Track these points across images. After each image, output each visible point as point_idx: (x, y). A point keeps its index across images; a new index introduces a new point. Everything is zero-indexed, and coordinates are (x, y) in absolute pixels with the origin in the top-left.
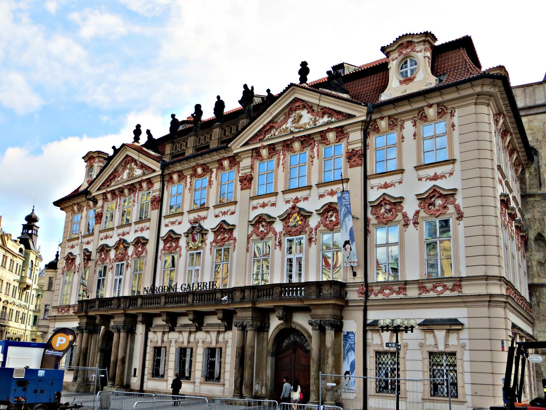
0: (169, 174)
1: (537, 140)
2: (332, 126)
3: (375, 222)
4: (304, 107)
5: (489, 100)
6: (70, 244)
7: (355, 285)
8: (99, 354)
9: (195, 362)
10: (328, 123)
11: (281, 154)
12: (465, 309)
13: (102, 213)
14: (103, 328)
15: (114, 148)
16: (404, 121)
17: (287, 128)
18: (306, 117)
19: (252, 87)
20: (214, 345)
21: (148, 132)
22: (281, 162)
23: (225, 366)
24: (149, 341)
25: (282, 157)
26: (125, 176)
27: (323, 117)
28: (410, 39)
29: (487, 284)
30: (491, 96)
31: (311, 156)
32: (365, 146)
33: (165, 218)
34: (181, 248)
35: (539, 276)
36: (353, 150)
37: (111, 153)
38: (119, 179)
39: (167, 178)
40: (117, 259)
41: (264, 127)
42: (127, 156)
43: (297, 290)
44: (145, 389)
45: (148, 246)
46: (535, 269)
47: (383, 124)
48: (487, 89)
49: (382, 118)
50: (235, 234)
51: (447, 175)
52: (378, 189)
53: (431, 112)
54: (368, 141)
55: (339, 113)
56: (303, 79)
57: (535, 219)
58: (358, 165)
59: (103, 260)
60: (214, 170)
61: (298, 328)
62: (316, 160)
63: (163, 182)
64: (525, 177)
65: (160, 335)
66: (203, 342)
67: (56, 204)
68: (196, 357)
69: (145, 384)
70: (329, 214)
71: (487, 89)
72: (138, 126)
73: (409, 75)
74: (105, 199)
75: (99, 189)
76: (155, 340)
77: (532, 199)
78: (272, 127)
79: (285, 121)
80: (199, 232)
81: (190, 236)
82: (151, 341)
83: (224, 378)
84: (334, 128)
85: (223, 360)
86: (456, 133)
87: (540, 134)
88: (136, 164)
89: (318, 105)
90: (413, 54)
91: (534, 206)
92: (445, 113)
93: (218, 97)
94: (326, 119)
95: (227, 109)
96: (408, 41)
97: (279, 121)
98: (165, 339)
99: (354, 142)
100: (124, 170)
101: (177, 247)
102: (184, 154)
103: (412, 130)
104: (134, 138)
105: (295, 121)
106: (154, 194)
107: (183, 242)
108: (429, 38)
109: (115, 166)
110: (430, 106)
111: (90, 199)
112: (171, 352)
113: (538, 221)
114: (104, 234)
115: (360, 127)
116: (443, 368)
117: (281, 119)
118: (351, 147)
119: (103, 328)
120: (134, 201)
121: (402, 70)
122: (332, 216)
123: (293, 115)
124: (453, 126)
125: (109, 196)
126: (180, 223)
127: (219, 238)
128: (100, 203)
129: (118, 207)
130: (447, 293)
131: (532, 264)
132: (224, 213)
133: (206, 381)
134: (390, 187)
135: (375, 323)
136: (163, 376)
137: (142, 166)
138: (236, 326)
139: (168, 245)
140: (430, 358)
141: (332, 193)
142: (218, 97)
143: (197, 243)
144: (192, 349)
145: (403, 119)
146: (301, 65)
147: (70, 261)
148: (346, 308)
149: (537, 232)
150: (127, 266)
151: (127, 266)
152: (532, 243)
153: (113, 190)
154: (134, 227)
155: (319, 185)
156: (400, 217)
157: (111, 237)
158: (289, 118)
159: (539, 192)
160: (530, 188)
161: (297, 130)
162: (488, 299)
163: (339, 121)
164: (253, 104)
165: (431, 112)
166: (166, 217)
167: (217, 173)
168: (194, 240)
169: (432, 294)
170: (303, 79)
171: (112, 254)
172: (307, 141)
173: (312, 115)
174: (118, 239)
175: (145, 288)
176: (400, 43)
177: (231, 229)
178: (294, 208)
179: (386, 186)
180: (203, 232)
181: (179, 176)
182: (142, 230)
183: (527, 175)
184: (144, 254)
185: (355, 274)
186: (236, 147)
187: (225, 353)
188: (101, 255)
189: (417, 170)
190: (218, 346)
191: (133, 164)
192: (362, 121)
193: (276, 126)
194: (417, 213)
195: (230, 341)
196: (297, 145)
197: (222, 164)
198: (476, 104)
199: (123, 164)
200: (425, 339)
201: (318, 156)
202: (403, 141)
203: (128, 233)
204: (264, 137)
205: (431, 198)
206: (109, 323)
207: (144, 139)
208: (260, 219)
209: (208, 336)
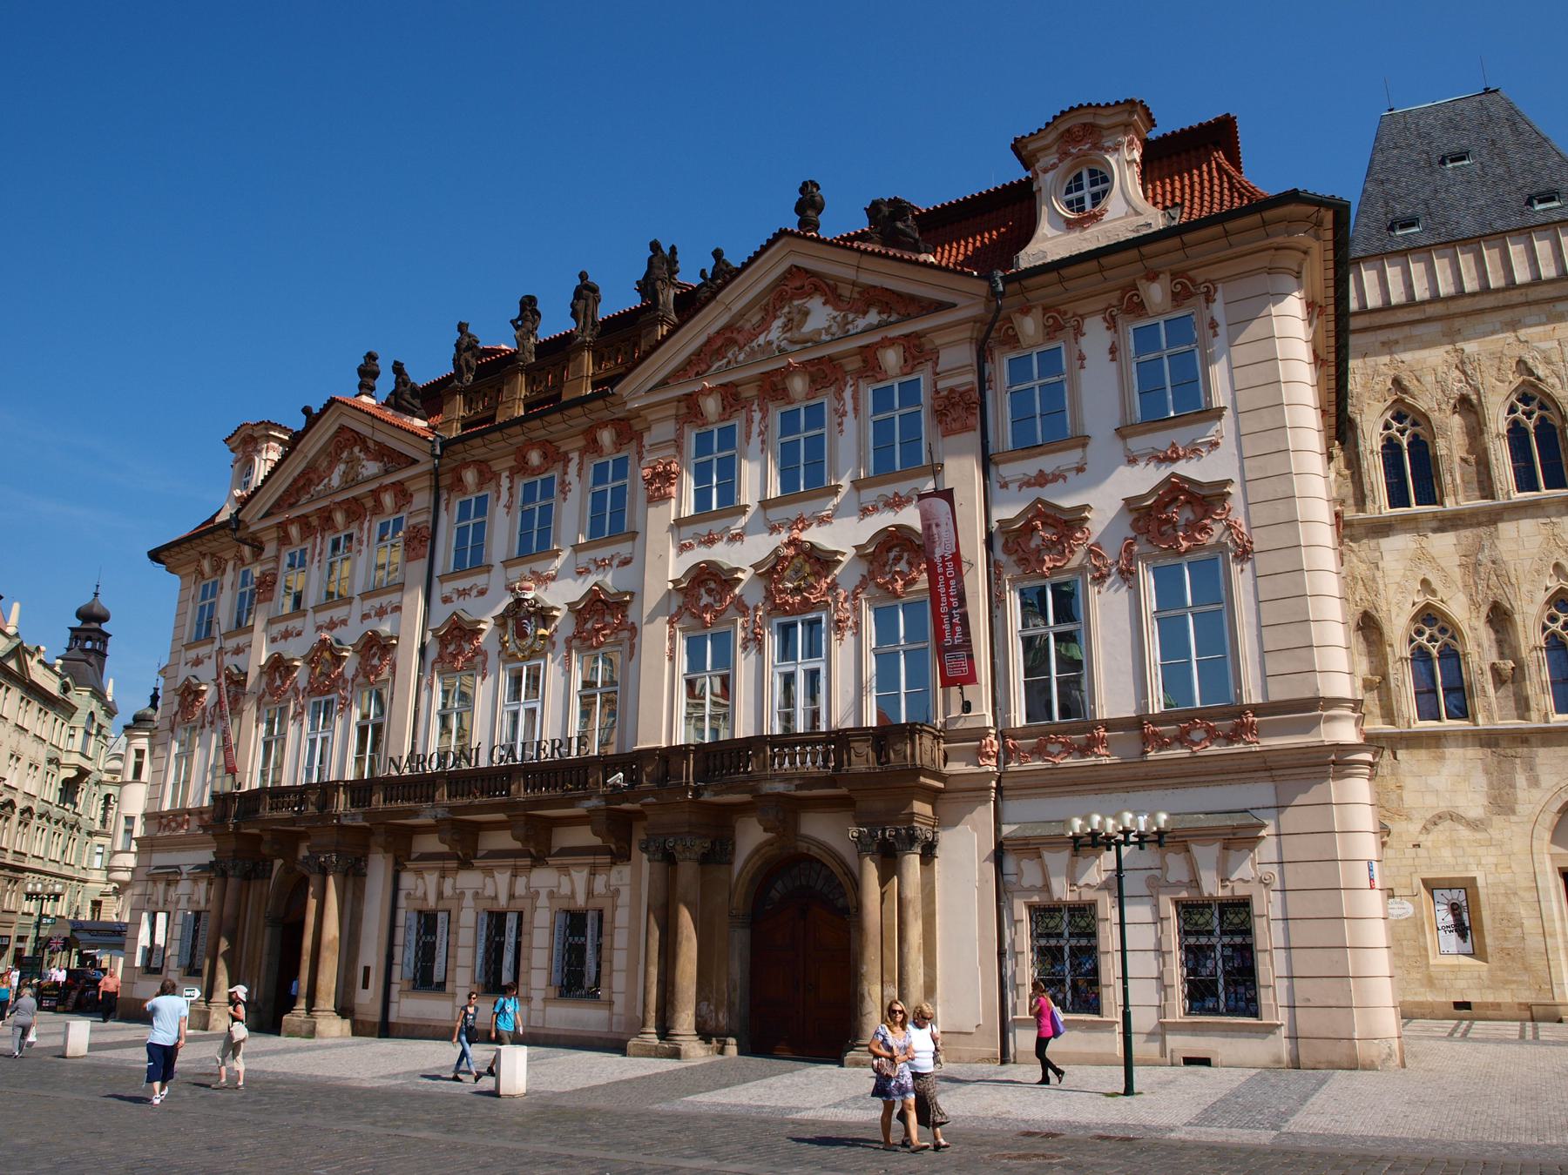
0: (453, 469)
2: (894, 332)
3: (1018, 571)
4: (817, 289)
6: (192, 654)
8: (268, 931)
9: (530, 947)
10: (879, 326)
11: (755, 407)
13: (275, 575)
14: (278, 863)
15: (306, 411)
16: (1083, 317)
17: (770, 343)
18: (820, 316)
19: (673, 249)
20: (581, 901)
21: (398, 368)
22: (755, 429)
23: (611, 955)
24: (402, 894)
25: (757, 416)
26: (336, 480)
27: (865, 313)
28: (1088, 119)
31: (836, 410)
32: (983, 382)
33: (442, 582)
34: (485, 654)
36: (951, 390)
37: (299, 423)
38: (321, 487)
39: (446, 480)
41: (709, 341)
42: (342, 428)
43: (803, 755)
44: (393, 1018)
47: (1029, 326)
49: (1025, 310)
52: (1020, 487)
53: (1156, 293)
54: (988, 367)
55: (912, 299)
56: (807, 223)
58: (966, 428)
60: (575, 456)
61: (814, 851)
62: (849, 421)
63: (436, 491)
65: (431, 879)
66: (551, 895)
67: (155, 556)
68: (530, 934)
69: (394, 1008)
70: (892, 555)
72: (371, 357)
73: (1088, 207)
74: (284, 540)
75: (267, 515)
76: (420, 893)
78: (733, 342)
79: (764, 325)
80: (534, 614)
81: (510, 623)
82: (409, 894)
83: (610, 987)
84: (898, 338)
85: (605, 940)
88: (365, 449)
89: (854, 284)
90: (1095, 154)
92: (1192, 295)
93: (583, 276)
94: (873, 317)
95: (606, 310)
96: (1085, 125)
97: (748, 326)
98: (448, 891)
100: (331, 468)
102: (493, 418)
104: (361, 386)
105: (786, 327)
106: (413, 521)
109: (310, 455)
111: (244, 542)
112: (463, 921)
115: (968, 334)
116: (1214, 940)
117: (754, 320)
118: (941, 385)
119: (278, 863)
120: (360, 542)
121: (1070, 196)
122: (897, 560)
123: (786, 310)
124: (1213, 325)
125: (294, 531)
126: (482, 593)
127: (589, 626)
128: (270, 549)
129: (317, 558)
133: (561, 995)
134: (1052, 481)
136: (441, 986)
138: (645, 850)
139: (451, 648)
141: (897, 503)
142: (583, 276)
143: (529, 641)
144: (520, 915)
145: (1080, 312)
146: (802, 191)
147: (190, 698)
149: (1361, 609)
153: (305, 516)
154: (357, 608)
157: (299, 634)
158: (775, 318)
163: (906, 318)
164: (667, 297)
166: (445, 578)
167: (581, 464)
168: (521, 634)
170: (807, 223)
173: (836, 308)
175: (392, 759)
176: (1063, 128)
178: (793, 542)
179: (1042, 479)
180: (544, 615)
181: (481, 473)
185: (967, 707)
186: (635, 392)
187: (613, 921)
188: (273, 680)
190: (592, 903)
191: (356, 450)
192: (975, 320)
193: (740, 338)
195: (625, 897)
197: (595, 441)
199: (331, 449)
201: (856, 410)
202: (1082, 367)
203: (344, 622)
204: (710, 367)
205: (1167, 505)
206: (296, 851)
207: (386, 383)
209: (565, 880)
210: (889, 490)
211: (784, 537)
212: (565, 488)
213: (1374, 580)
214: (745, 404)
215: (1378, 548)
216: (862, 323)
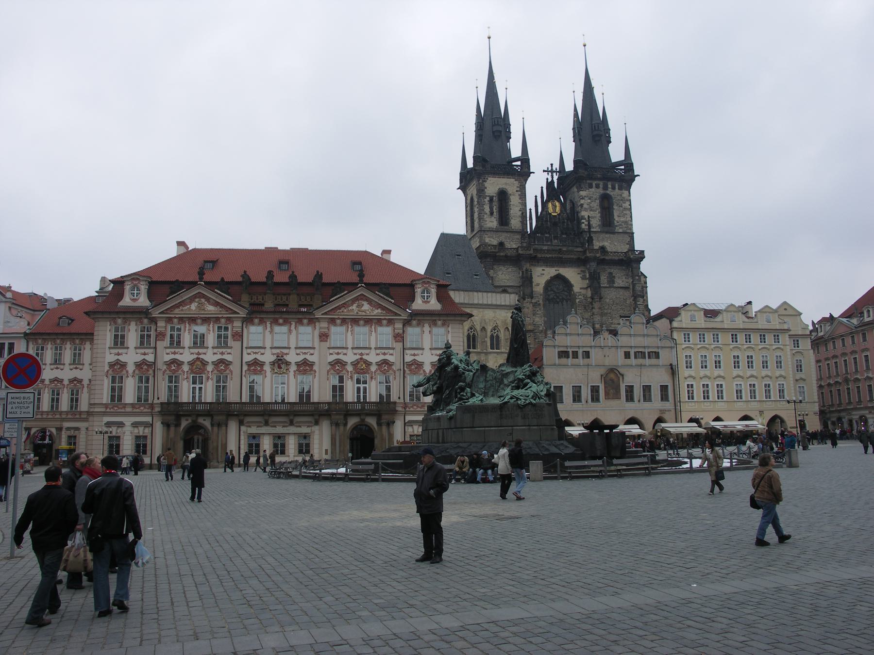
7: (400, 403)
18: (366, 306)
40: (192, 371)
45: (231, 367)
47: (414, 322)
50: (315, 368)
53: (439, 323)
59: (175, 371)
99: (399, 329)
100: (191, 303)
101: (262, 370)
102: (263, 305)
103: (429, 329)
107: (267, 368)
114: (173, 350)
126: (262, 354)
128: (161, 324)
132: (305, 353)
135: (410, 422)
137: (217, 304)
150: (208, 378)
151: (208, 378)
155: (376, 348)
156: (422, 372)
161: (360, 313)
168: (280, 367)
170: (361, 281)
171: (186, 368)
172: (368, 321)
174: (195, 356)
177: (311, 365)
178: (361, 359)
179: (414, 355)
180: (288, 364)
182: (222, 353)
184: (228, 371)
186: (318, 314)
191: (203, 300)
196: (362, 322)
208: (338, 362)
210: (383, 351)
211: (358, 357)
212: (290, 331)
214: (347, 323)
216: (377, 311)
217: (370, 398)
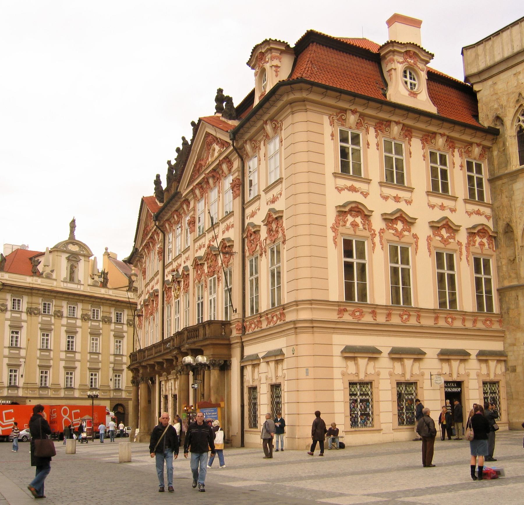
1: (502, 106)
5: (305, 106)
12: (284, 339)
29: (297, 310)
30: (304, 101)
35: (510, 277)
41: (195, 166)
46: (505, 269)
48: (292, 97)
51: (279, 196)
57: (503, 206)
63: (163, 232)
64: (492, 156)
71: (292, 97)
72: (158, 176)
77: (500, 182)
78: (201, 166)
86: (283, 148)
87: (505, 98)
91: (501, 191)
108: (272, 46)
110: (266, 123)
113: (506, 209)
130: (279, 323)
131: (501, 263)
140: (272, 391)
148: (232, 346)
152: (501, 236)
156: (258, 247)
159: (506, 172)
160: (499, 168)
162: (292, 326)
165: (269, 128)
169: (272, 325)
183: (495, 153)
189: (266, 193)
194: (266, 239)
198: (293, 113)
200: (347, 367)
213: (511, 206)
215: (512, 190)
217: (462, 305)
